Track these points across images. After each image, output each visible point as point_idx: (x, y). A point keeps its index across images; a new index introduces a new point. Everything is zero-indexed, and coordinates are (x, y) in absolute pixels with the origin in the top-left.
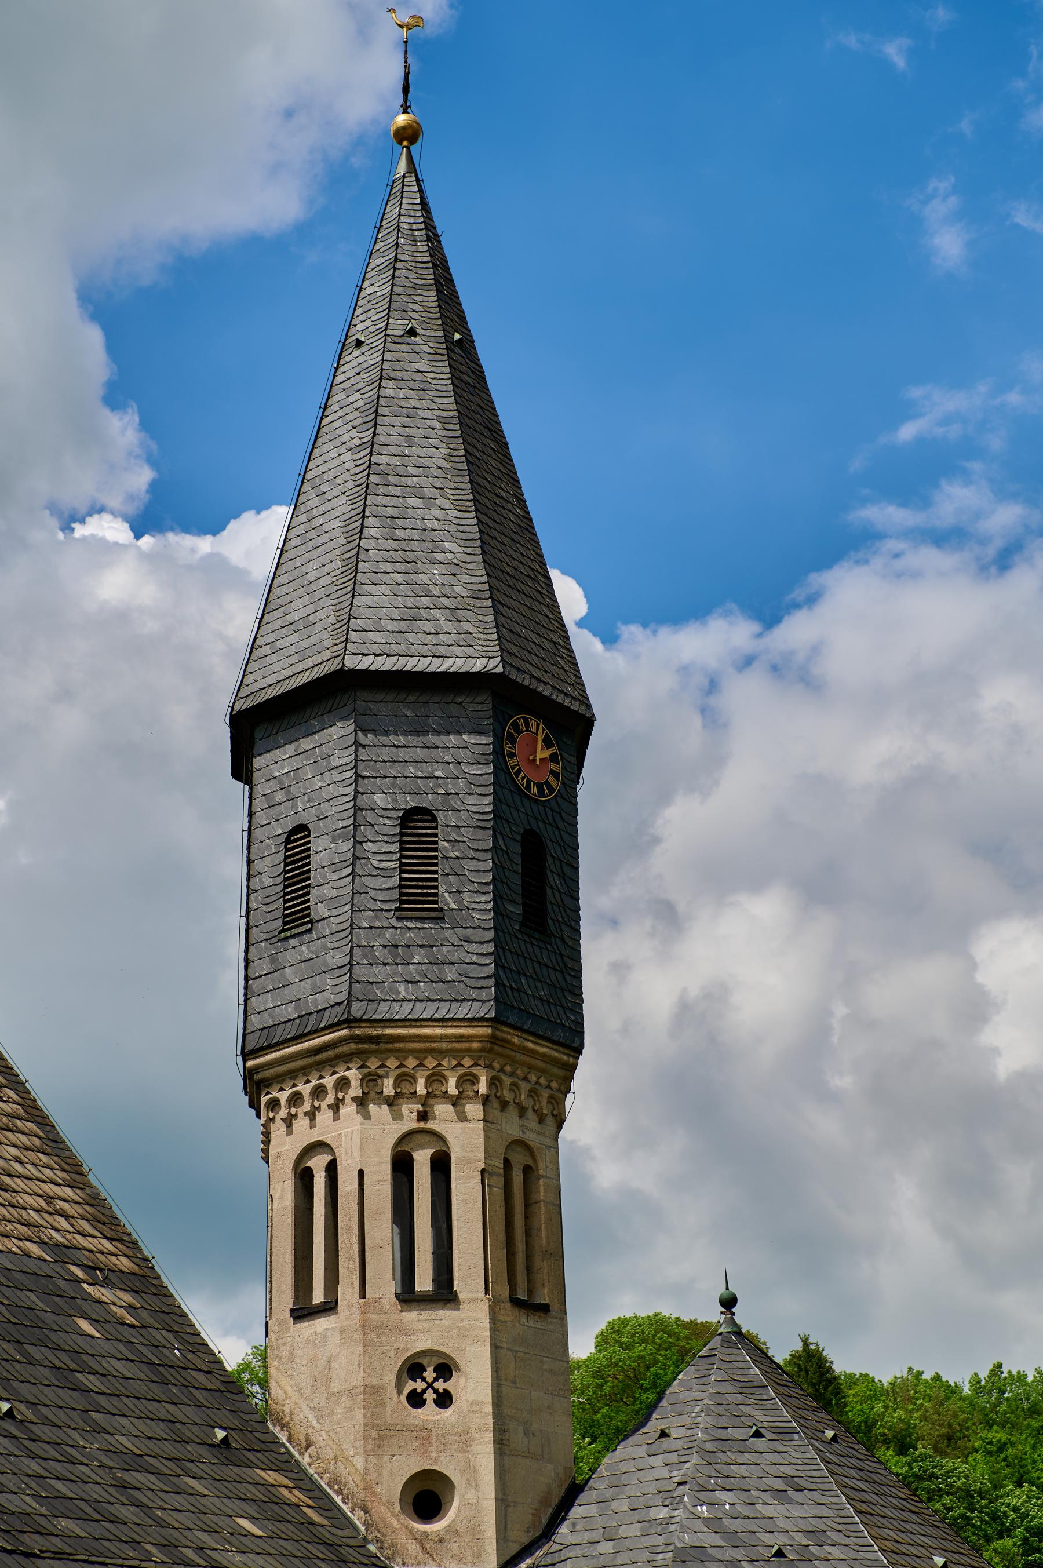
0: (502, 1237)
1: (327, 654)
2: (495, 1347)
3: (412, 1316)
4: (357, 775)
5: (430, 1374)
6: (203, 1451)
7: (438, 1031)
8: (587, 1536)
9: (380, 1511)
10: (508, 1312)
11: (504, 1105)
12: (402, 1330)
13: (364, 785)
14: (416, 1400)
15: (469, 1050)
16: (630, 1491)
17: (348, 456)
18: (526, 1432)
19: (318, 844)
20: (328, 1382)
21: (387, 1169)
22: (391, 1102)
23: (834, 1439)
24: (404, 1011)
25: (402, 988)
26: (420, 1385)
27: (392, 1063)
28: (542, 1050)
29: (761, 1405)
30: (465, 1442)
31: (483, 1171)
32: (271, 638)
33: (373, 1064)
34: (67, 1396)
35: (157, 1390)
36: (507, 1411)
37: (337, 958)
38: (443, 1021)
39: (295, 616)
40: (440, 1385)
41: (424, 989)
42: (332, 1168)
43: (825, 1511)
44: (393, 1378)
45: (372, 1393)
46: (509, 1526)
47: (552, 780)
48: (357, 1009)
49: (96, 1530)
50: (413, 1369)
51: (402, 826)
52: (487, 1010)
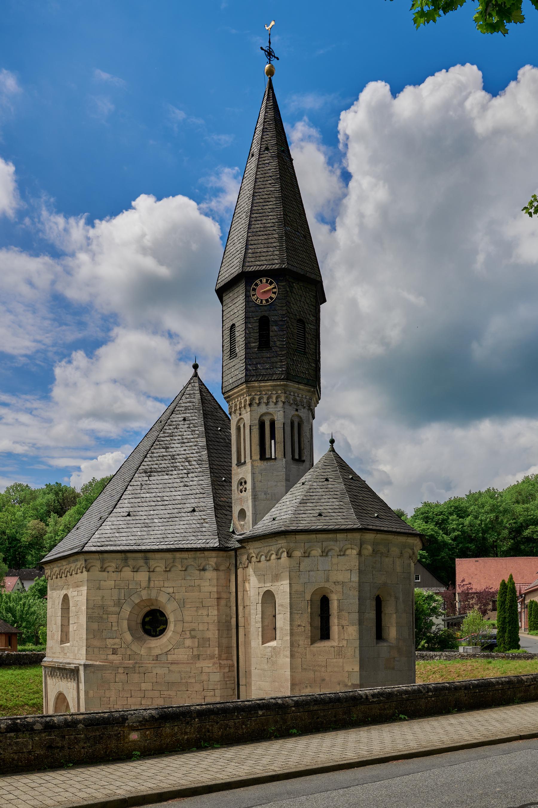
18: (265, 494)
31: (250, 426)
36: (257, 489)
40: (245, 486)
44: (236, 487)
46: (257, 519)
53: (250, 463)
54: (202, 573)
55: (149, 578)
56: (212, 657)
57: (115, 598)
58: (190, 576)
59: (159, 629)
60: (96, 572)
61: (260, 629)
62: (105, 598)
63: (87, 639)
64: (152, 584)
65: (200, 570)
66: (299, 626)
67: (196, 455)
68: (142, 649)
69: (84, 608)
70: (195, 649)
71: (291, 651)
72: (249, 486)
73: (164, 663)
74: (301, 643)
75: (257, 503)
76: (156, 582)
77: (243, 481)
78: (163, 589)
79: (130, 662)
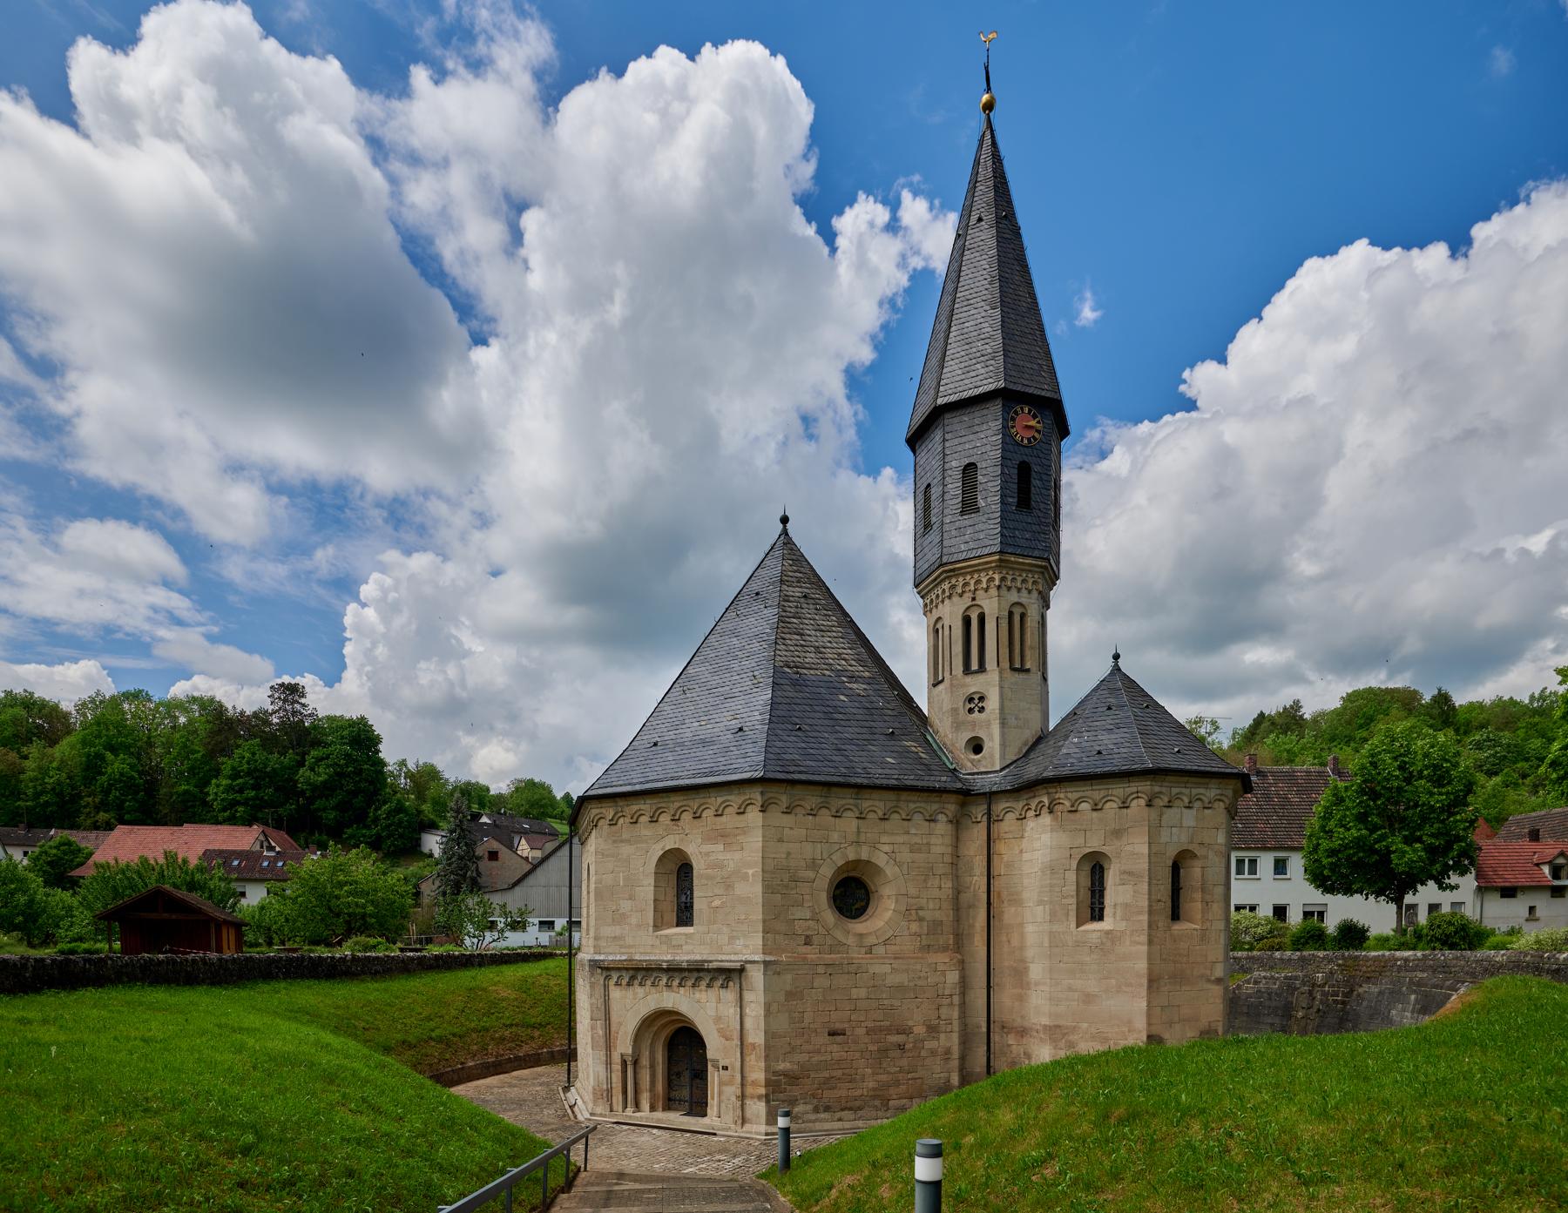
0: (1007, 643)
2: (1001, 687)
3: (969, 679)
5: (976, 701)
6: (882, 737)
10: (1008, 673)
12: (964, 685)
14: (971, 711)
18: (1016, 719)
19: (933, 490)
22: (961, 595)
26: (973, 706)
27: (961, 579)
30: (988, 724)
34: (827, 722)
40: (980, 705)
44: (962, 704)
48: (945, 560)
50: (971, 700)
54: (932, 824)
59: (856, 906)
64: (862, 839)
65: (929, 821)
68: (850, 937)
69: (754, 871)
70: (924, 937)
72: (993, 703)
73: (884, 958)
75: (1006, 730)
76: (868, 835)
77: (976, 697)
78: (877, 846)
79: (832, 956)
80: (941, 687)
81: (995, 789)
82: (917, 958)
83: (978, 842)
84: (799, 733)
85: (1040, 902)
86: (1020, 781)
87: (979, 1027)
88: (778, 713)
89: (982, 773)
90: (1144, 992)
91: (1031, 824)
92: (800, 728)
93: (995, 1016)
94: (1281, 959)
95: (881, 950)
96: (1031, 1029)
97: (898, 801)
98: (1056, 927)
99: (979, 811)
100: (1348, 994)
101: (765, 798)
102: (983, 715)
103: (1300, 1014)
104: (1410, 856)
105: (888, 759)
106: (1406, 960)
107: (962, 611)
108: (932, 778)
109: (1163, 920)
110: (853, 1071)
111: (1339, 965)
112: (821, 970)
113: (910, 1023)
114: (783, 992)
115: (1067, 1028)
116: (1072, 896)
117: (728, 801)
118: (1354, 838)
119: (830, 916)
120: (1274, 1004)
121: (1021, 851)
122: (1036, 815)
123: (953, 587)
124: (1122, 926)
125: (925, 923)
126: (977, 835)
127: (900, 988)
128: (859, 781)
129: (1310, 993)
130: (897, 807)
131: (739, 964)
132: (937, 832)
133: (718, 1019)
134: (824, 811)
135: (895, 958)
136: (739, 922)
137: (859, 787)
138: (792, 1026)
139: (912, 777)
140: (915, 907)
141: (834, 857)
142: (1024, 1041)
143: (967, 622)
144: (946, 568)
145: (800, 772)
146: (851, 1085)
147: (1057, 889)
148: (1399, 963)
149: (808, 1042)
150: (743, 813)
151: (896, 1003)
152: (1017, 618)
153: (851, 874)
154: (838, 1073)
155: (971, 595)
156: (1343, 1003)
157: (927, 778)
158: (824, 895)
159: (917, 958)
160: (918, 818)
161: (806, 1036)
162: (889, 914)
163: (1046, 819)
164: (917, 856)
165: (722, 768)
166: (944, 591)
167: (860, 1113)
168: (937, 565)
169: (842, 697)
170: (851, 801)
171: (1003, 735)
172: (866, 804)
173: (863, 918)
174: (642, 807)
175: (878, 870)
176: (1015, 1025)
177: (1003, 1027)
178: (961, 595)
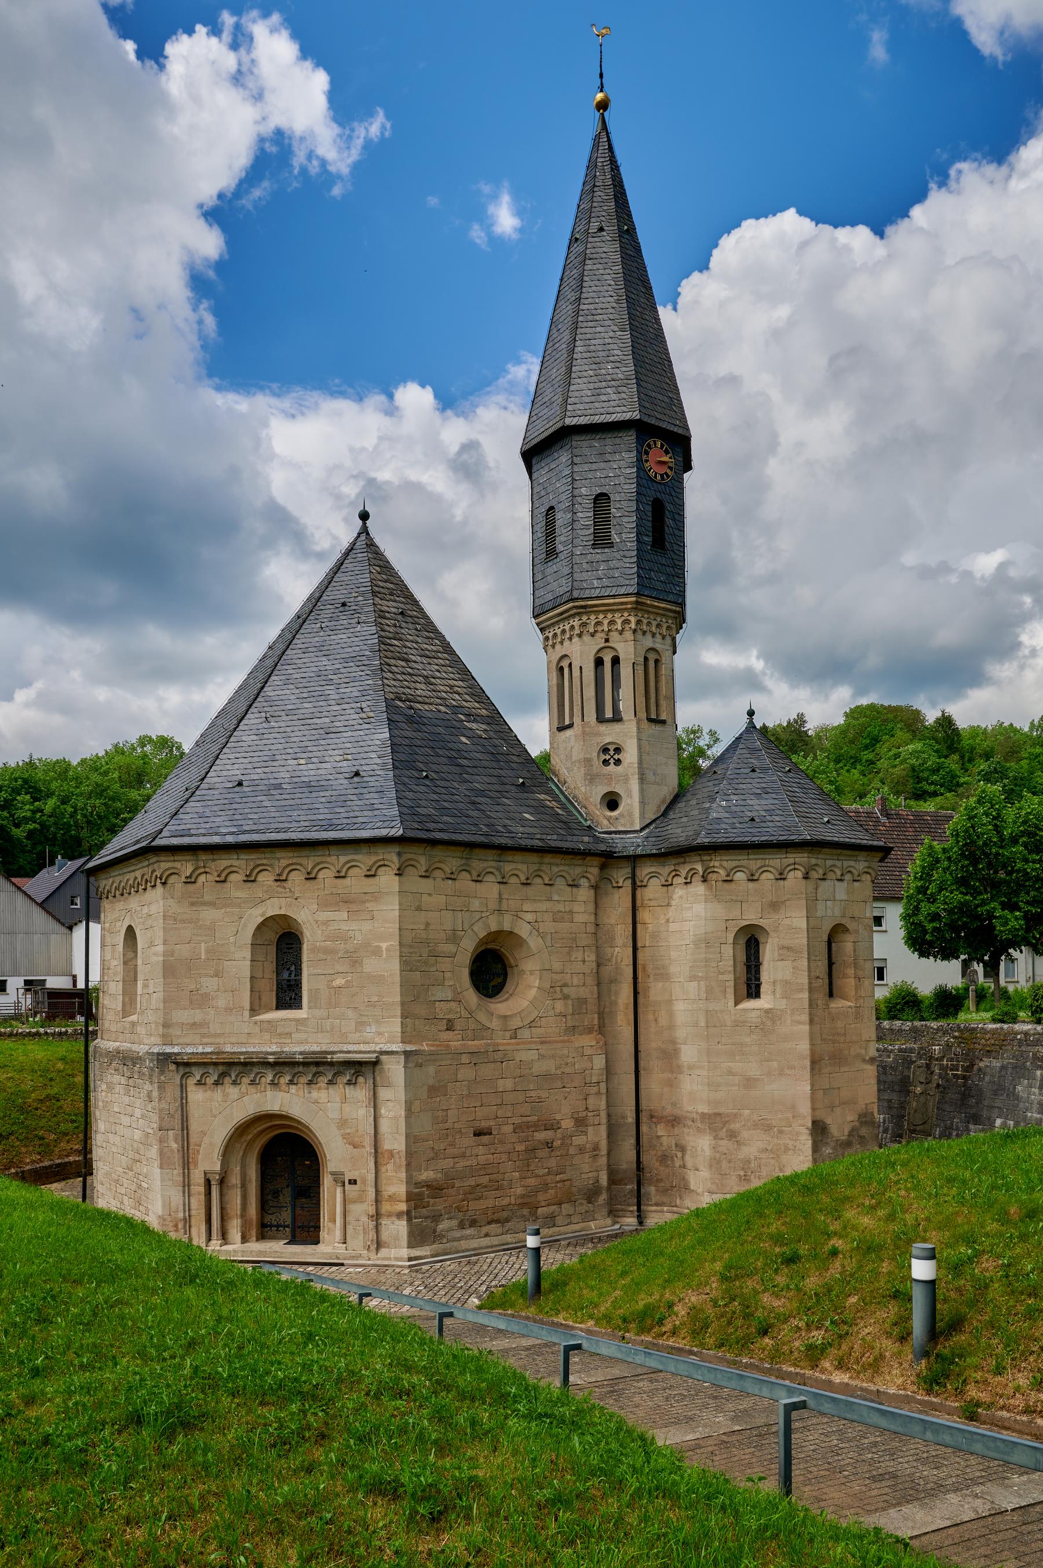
0: (643, 692)
1: (558, 418)
2: (639, 740)
3: (603, 728)
4: (574, 480)
5: (612, 753)
6: (512, 788)
7: (612, 601)
8: (679, 815)
9: (591, 808)
10: (645, 724)
11: (644, 633)
12: (598, 734)
13: (577, 484)
14: (606, 762)
15: (626, 609)
16: (697, 796)
17: (570, 307)
19: (559, 515)
20: (571, 756)
21: (592, 665)
22: (592, 635)
23: (789, 771)
24: (596, 593)
25: (595, 582)
26: (607, 757)
27: (593, 617)
28: (663, 605)
29: (757, 758)
30: (626, 779)
32: (536, 412)
33: (584, 618)
34: (453, 769)
35: (494, 764)
36: (645, 766)
37: (566, 570)
38: (614, 596)
39: (546, 399)
40: (616, 757)
41: (605, 581)
42: (570, 665)
43: (776, 802)
45: (588, 761)
47: (668, 471)
48: (576, 594)
49: (458, 820)
50: (605, 750)
51: (595, 503)
52: (633, 589)
53: (635, 723)
54: (575, 890)
55: (500, 894)
56: (590, 1031)
57: (448, 926)
58: (559, 895)
59: (492, 984)
60: (415, 883)
61: (732, 983)
62: (432, 927)
63: (403, 1004)
66: (818, 977)
67: (461, 683)
70: (569, 1017)
71: (810, 1014)
72: (630, 756)
73: (530, 1043)
74: (820, 1002)
75: (645, 786)
77: (612, 748)
78: (520, 914)
79: (476, 1042)
80: (569, 733)
81: (639, 851)
82: (563, 1042)
83: (620, 909)
84: (427, 782)
85: (693, 978)
86: (665, 845)
87: (624, 1117)
88: (403, 757)
89: (620, 832)
90: (807, 1074)
91: (679, 892)
92: (426, 776)
93: (644, 1104)
94: (891, 1030)
95: (525, 1034)
96: (686, 1118)
97: (541, 863)
98: (712, 1006)
99: (621, 875)
100: (969, 1069)
101: (403, 859)
102: (620, 769)
103: (919, 1090)
104: (1013, 923)
105: (527, 816)
106: (1026, 1034)
107: (594, 652)
108: (575, 838)
109: (821, 997)
110: (500, 1177)
111: (955, 1037)
112: (465, 1059)
113: (558, 1117)
114: (426, 1087)
115: (728, 1115)
116: (729, 972)
117: (354, 860)
118: (959, 902)
119: (471, 996)
120: (890, 1078)
121: (668, 921)
122: (686, 883)
123: (584, 625)
124: (782, 1004)
125: (570, 1002)
126: (619, 901)
127: (546, 1077)
128: (503, 841)
129: (928, 1066)
130: (539, 870)
131: (375, 1055)
132: (580, 898)
133: (343, 1123)
134: (464, 874)
135: (542, 1043)
136: (370, 1004)
137: (503, 849)
138: (435, 1127)
139: (555, 837)
140: (559, 984)
141: (475, 928)
142: (676, 1131)
143: (599, 662)
144: (576, 604)
145: (441, 830)
146: (498, 1193)
147: (714, 964)
148: (1019, 1037)
149: (452, 1145)
150: (374, 876)
151: (544, 1094)
152: (651, 664)
153: (489, 947)
154: (484, 1180)
155: (603, 635)
156: (964, 1077)
157: (569, 838)
158: (466, 972)
159: (563, 1042)
160: (560, 882)
161: (450, 1138)
162: (533, 992)
163: (698, 888)
164: (560, 925)
165: (345, 821)
166: (572, 628)
167: (508, 1225)
168: (565, 598)
169: (463, 739)
170: (493, 864)
171: (642, 791)
172: (508, 867)
173: (503, 995)
174: (235, 863)
175: (519, 941)
176: (665, 1114)
177: (652, 1117)
178: (592, 635)
